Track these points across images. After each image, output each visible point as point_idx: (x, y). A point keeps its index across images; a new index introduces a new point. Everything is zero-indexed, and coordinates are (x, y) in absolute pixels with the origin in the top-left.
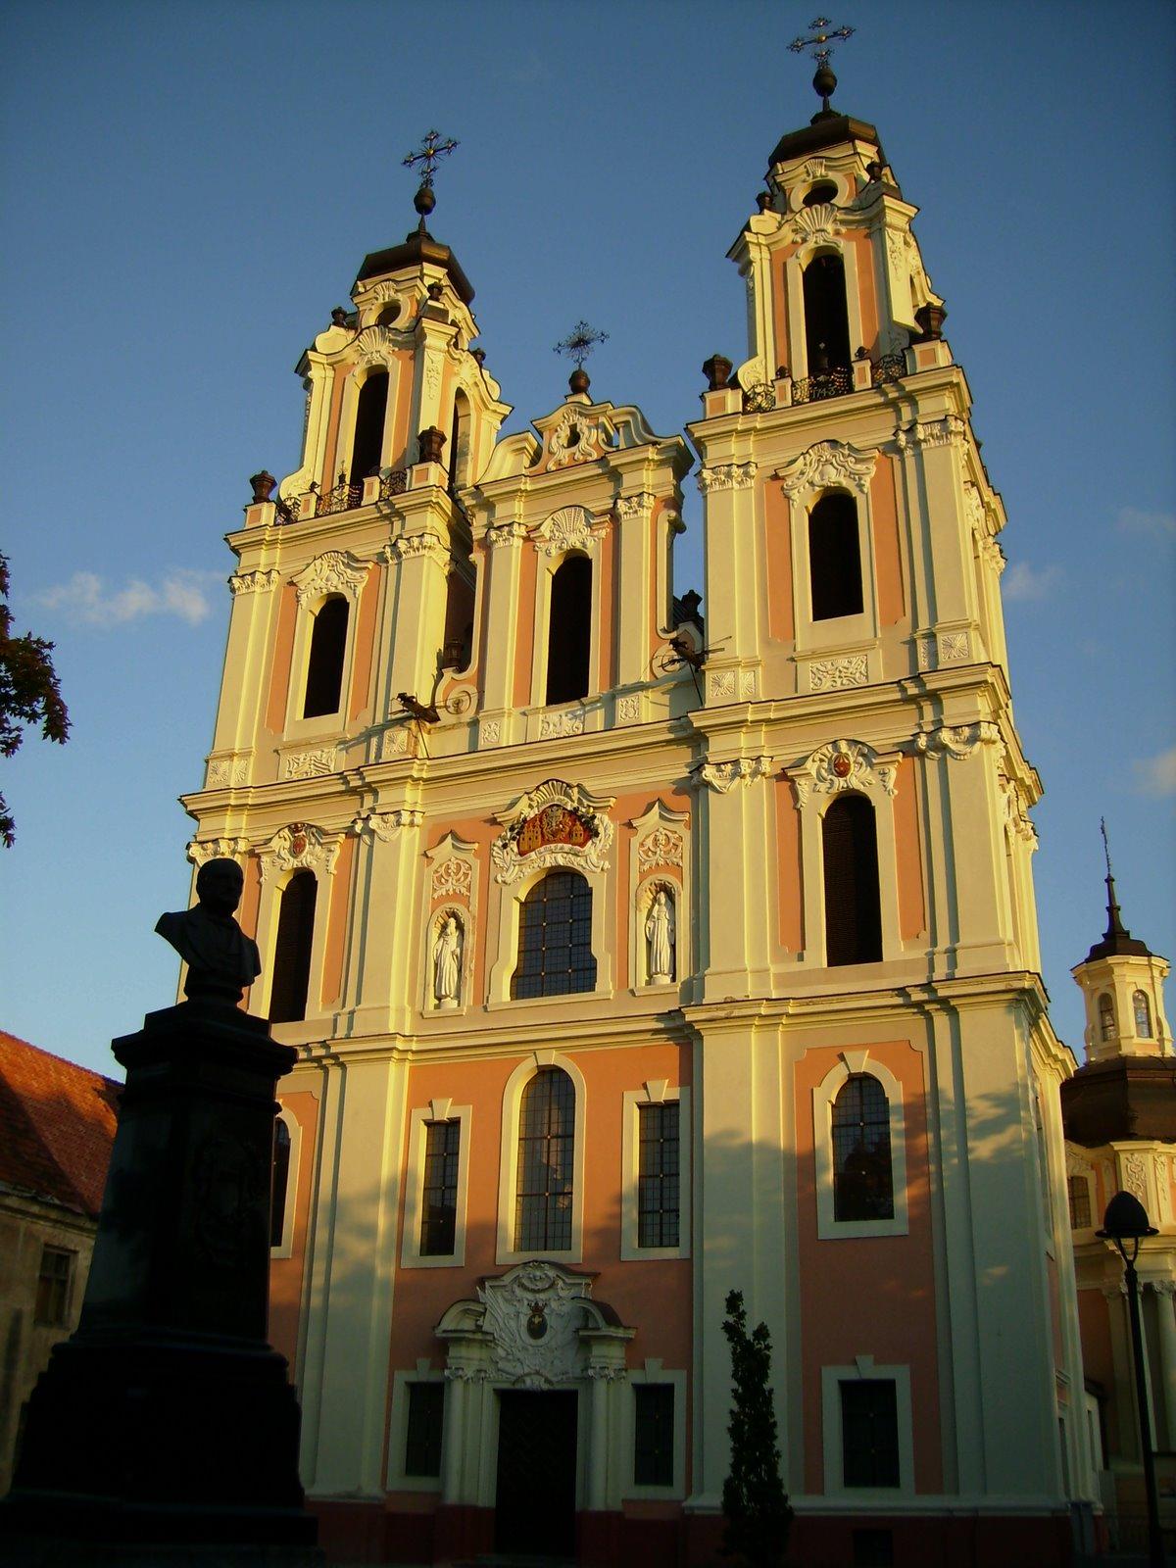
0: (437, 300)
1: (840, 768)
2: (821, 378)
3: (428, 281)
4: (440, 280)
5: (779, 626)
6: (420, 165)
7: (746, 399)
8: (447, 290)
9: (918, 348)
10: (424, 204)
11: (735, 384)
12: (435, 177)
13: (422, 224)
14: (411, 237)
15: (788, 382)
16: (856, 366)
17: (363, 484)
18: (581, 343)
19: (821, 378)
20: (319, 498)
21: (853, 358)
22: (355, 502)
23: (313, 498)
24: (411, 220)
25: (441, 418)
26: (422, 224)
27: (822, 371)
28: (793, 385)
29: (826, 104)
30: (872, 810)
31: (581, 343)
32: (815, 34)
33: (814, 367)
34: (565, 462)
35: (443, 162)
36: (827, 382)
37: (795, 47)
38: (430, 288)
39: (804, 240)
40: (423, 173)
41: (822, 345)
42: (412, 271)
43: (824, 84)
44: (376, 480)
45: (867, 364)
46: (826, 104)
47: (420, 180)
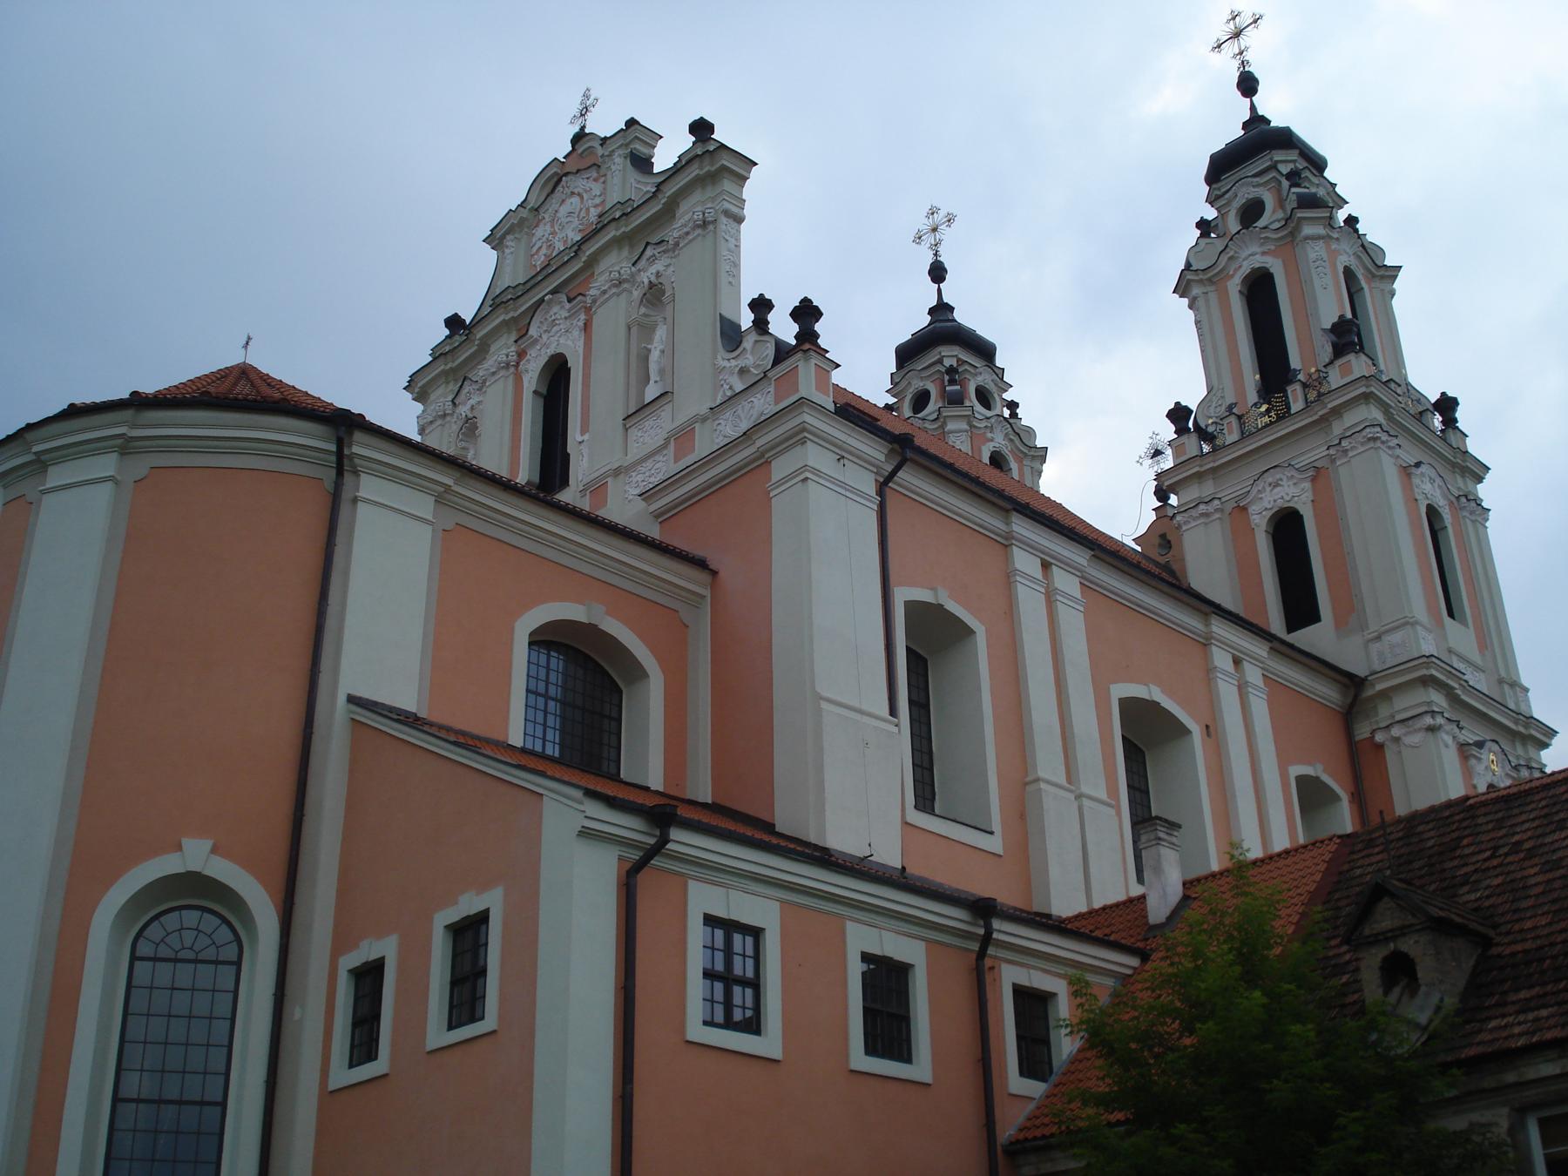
0: (1298, 186)
3: (1285, 169)
4: (1294, 161)
6: (1231, 48)
8: (1307, 174)
10: (1248, 85)
12: (1248, 56)
13: (1253, 108)
14: (1245, 125)
17: (1285, 391)
20: (1239, 417)
22: (1285, 414)
23: (1233, 419)
24: (1240, 109)
25: (1342, 306)
26: (1253, 108)
35: (1248, 39)
38: (1289, 176)
40: (1235, 56)
42: (1262, 163)
44: (1297, 387)
47: (1236, 63)
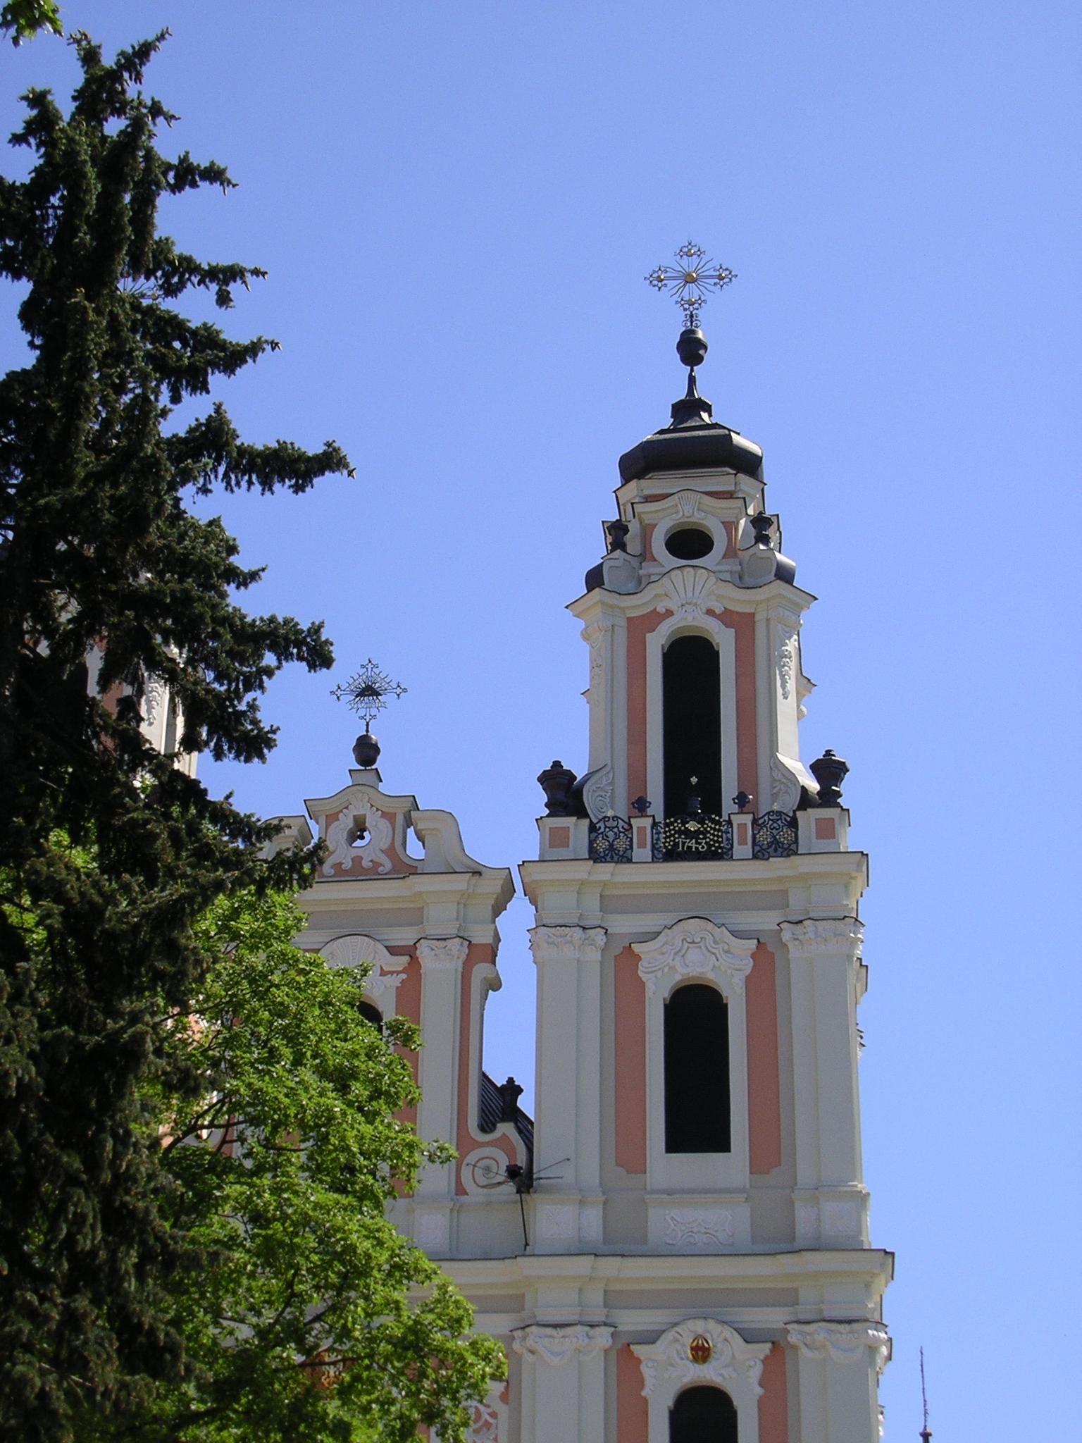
1: (701, 1353)
2: (692, 826)
5: (629, 1157)
7: (593, 828)
9: (814, 814)
11: (581, 812)
15: (647, 822)
16: (736, 820)
18: (368, 691)
19: (692, 826)
21: (728, 806)
27: (694, 816)
28: (655, 824)
29: (692, 381)
30: (735, 1413)
31: (368, 691)
32: (689, 265)
33: (676, 804)
34: (348, 864)
36: (698, 832)
37: (657, 280)
39: (669, 613)
41: (694, 780)
43: (691, 350)
45: (747, 819)
46: (692, 381)
